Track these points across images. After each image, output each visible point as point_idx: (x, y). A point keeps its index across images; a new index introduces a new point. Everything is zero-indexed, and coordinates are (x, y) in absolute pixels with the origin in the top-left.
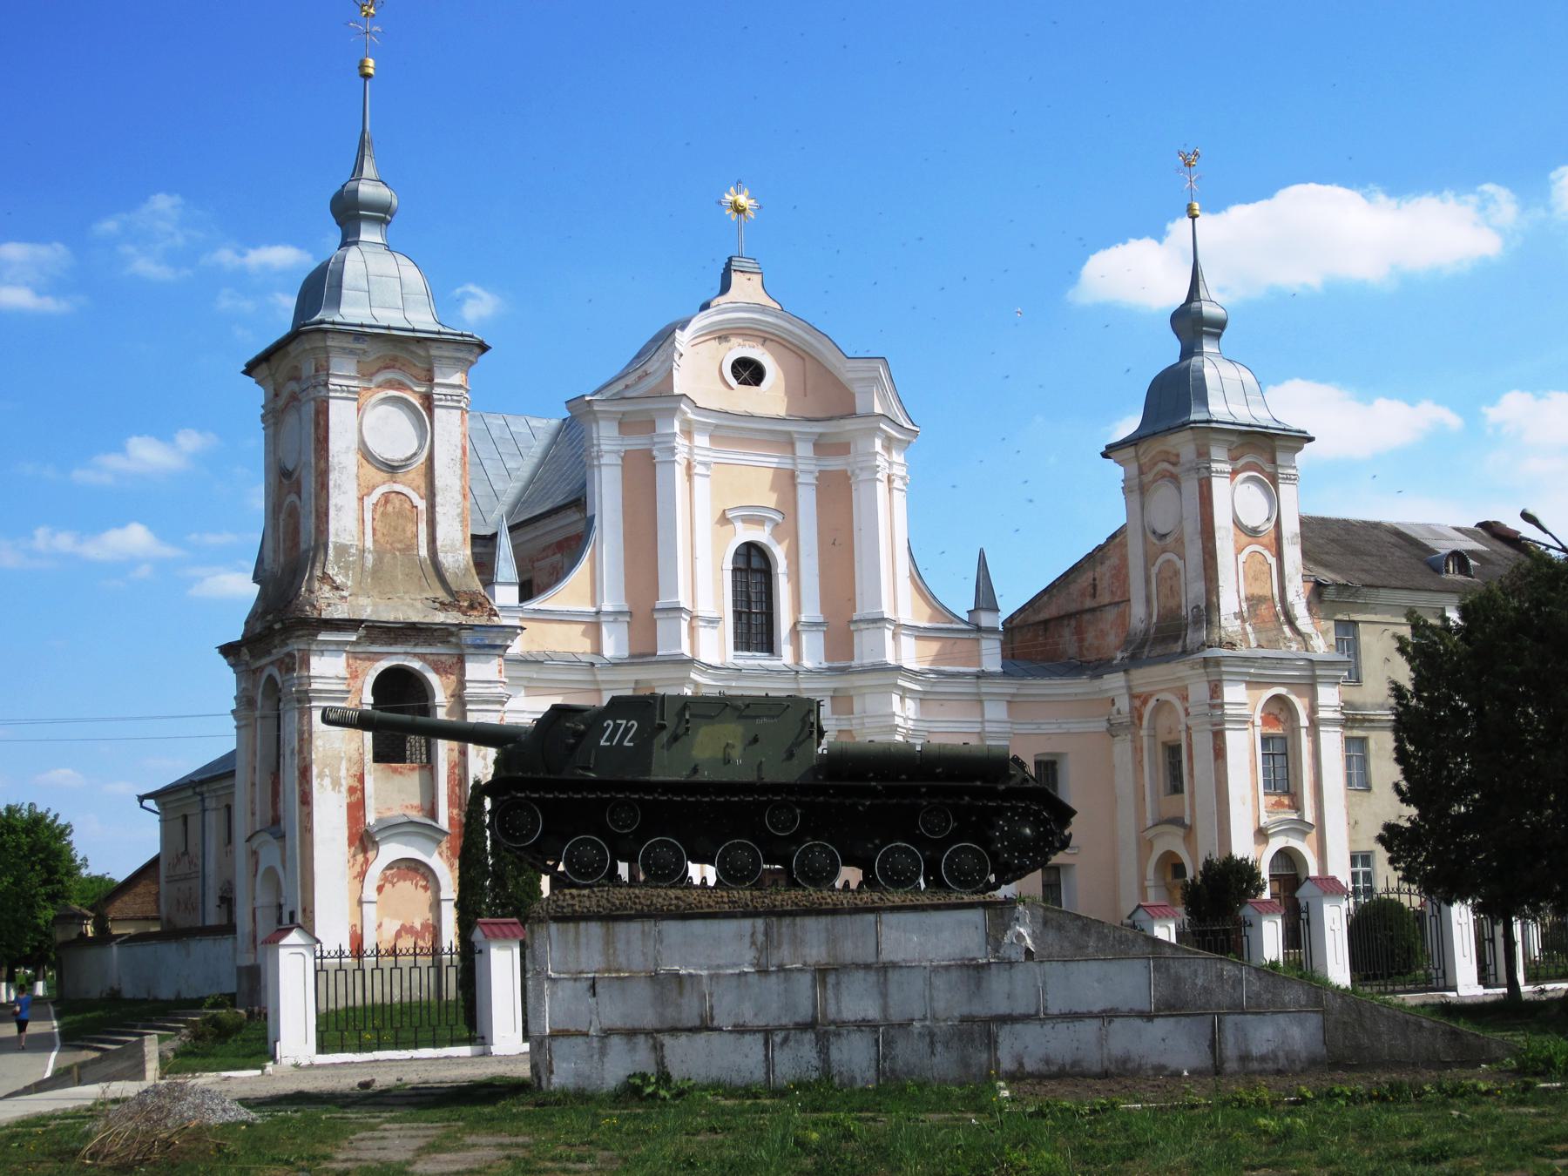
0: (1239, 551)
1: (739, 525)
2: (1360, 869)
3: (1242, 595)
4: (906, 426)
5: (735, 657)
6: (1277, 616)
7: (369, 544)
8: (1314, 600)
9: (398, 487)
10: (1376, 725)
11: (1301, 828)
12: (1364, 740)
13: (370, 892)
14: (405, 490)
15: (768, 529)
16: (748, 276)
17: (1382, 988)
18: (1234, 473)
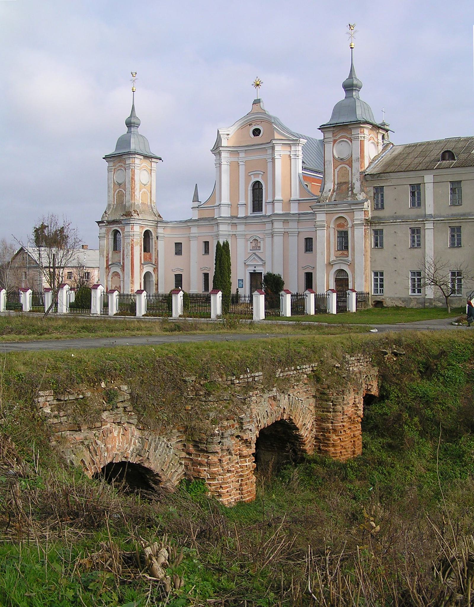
0: (335, 168)
1: (252, 176)
2: (379, 277)
3: (336, 183)
4: (295, 139)
5: (253, 214)
6: (348, 189)
7: (115, 203)
8: (364, 181)
9: (120, 189)
10: (386, 224)
11: (346, 262)
12: (382, 231)
13: (110, 279)
14: (122, 190)
15: (260, 176)
16: (257, 104)
17: (78, 312)
18: (335, 141)
